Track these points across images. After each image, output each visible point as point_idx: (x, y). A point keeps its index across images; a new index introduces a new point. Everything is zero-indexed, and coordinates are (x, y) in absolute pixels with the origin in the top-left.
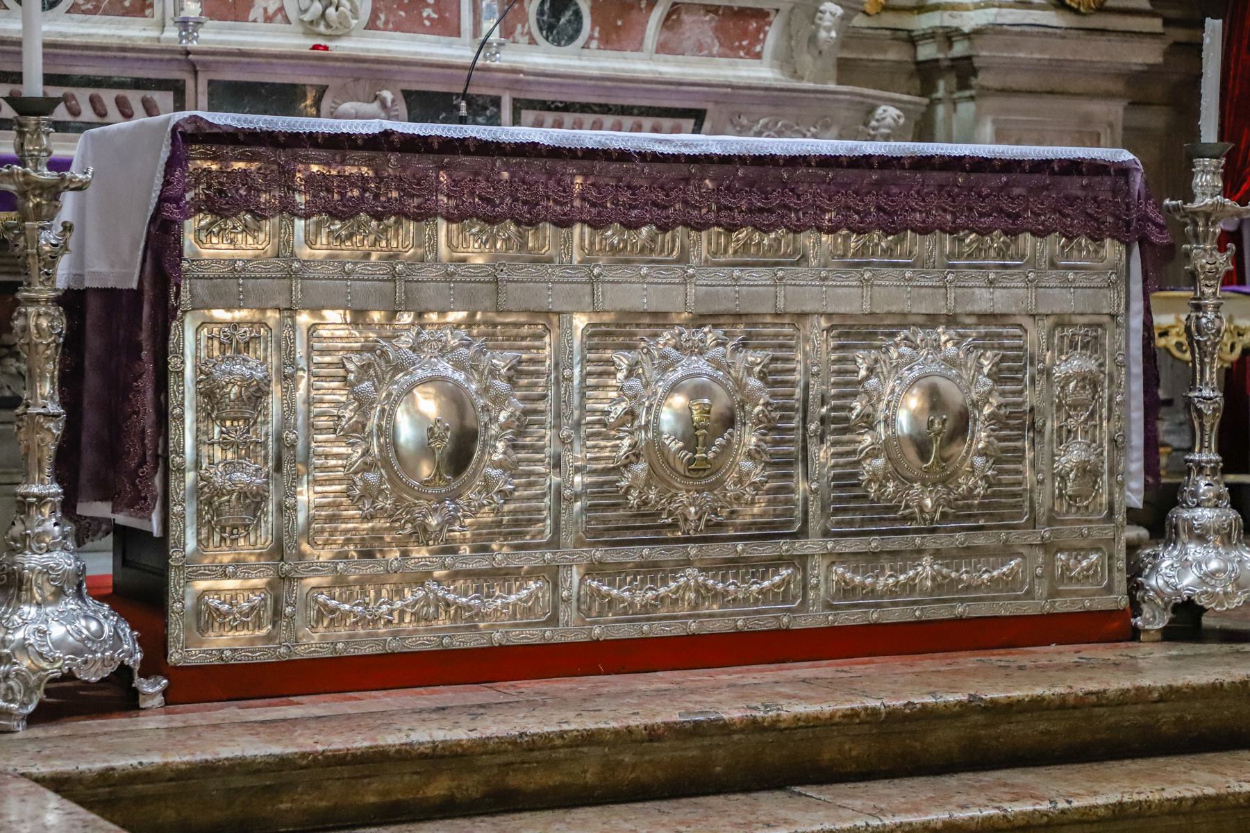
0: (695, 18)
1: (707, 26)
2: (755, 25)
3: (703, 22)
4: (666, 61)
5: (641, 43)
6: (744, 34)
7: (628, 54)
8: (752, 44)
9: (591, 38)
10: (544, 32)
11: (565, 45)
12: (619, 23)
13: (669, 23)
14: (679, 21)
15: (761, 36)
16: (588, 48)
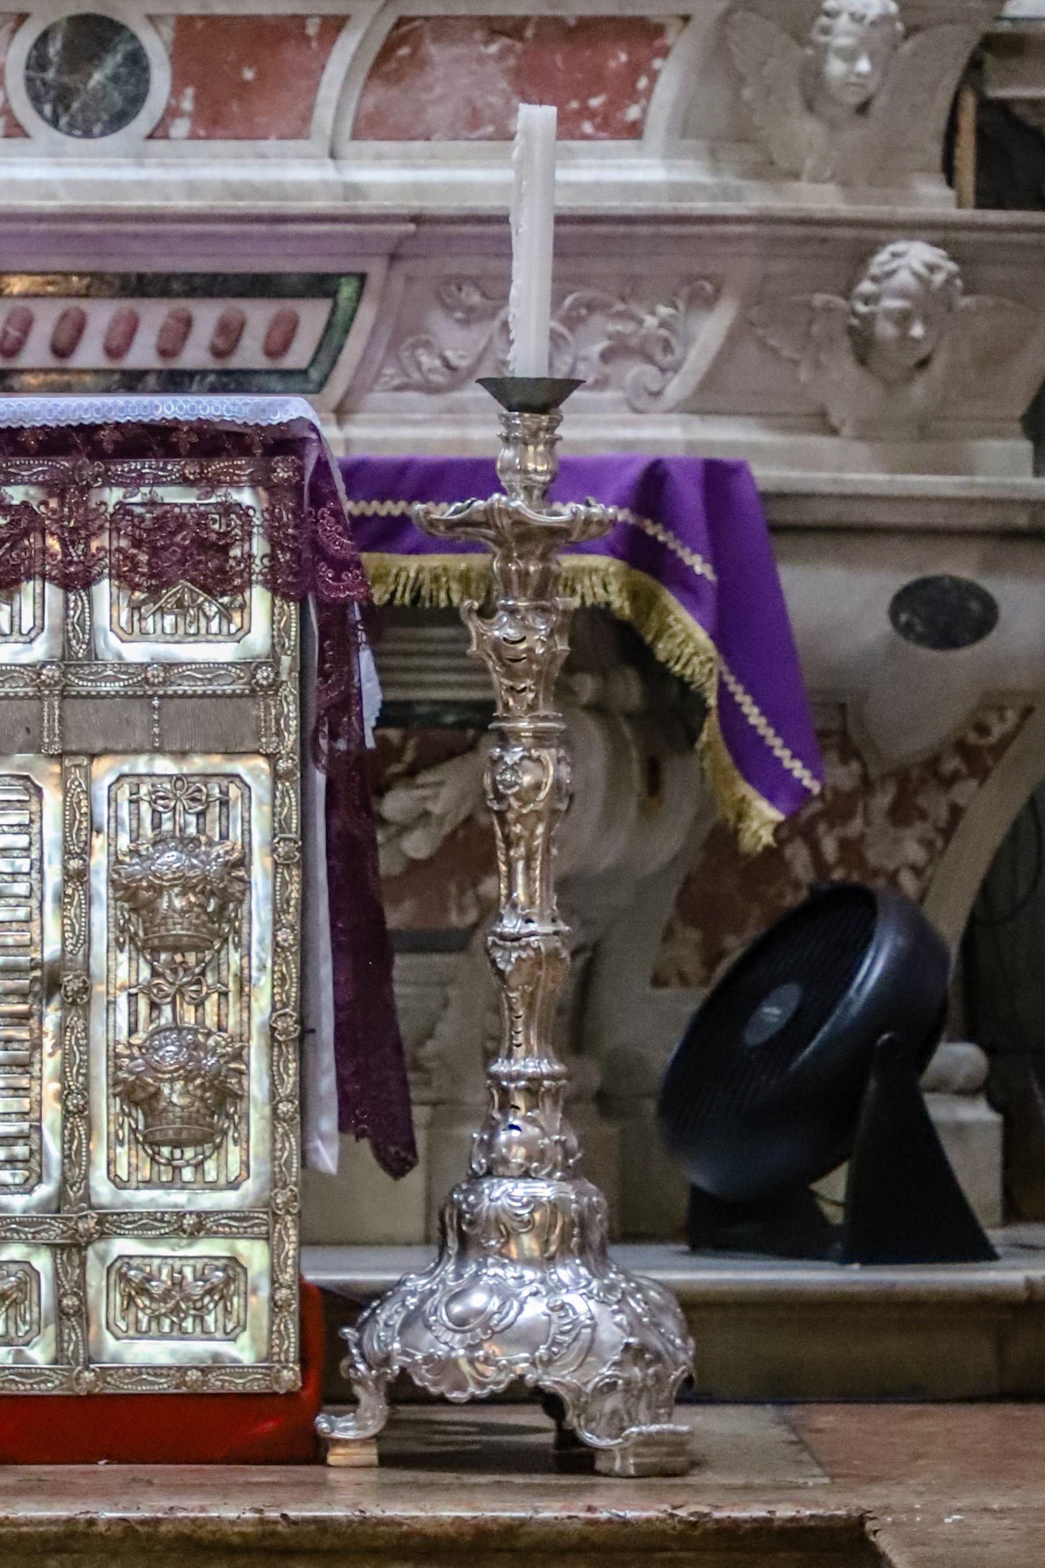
0: (458, 50)
1: (492, 68)
2: (623, 57)
3: (481, 59)
4: (379, 157)
5: (306, 118)
6: (597, 82)
7: (269, 145)
8: (616, 104)
9: (172, 113)
10: (48, 109)
11: (103, 134)
12: (249, 75)
13: (392, 65)
14: (418, 62)
15: (643, 83)
16: (166, 137)
